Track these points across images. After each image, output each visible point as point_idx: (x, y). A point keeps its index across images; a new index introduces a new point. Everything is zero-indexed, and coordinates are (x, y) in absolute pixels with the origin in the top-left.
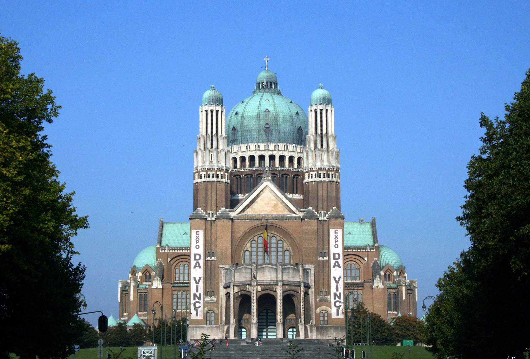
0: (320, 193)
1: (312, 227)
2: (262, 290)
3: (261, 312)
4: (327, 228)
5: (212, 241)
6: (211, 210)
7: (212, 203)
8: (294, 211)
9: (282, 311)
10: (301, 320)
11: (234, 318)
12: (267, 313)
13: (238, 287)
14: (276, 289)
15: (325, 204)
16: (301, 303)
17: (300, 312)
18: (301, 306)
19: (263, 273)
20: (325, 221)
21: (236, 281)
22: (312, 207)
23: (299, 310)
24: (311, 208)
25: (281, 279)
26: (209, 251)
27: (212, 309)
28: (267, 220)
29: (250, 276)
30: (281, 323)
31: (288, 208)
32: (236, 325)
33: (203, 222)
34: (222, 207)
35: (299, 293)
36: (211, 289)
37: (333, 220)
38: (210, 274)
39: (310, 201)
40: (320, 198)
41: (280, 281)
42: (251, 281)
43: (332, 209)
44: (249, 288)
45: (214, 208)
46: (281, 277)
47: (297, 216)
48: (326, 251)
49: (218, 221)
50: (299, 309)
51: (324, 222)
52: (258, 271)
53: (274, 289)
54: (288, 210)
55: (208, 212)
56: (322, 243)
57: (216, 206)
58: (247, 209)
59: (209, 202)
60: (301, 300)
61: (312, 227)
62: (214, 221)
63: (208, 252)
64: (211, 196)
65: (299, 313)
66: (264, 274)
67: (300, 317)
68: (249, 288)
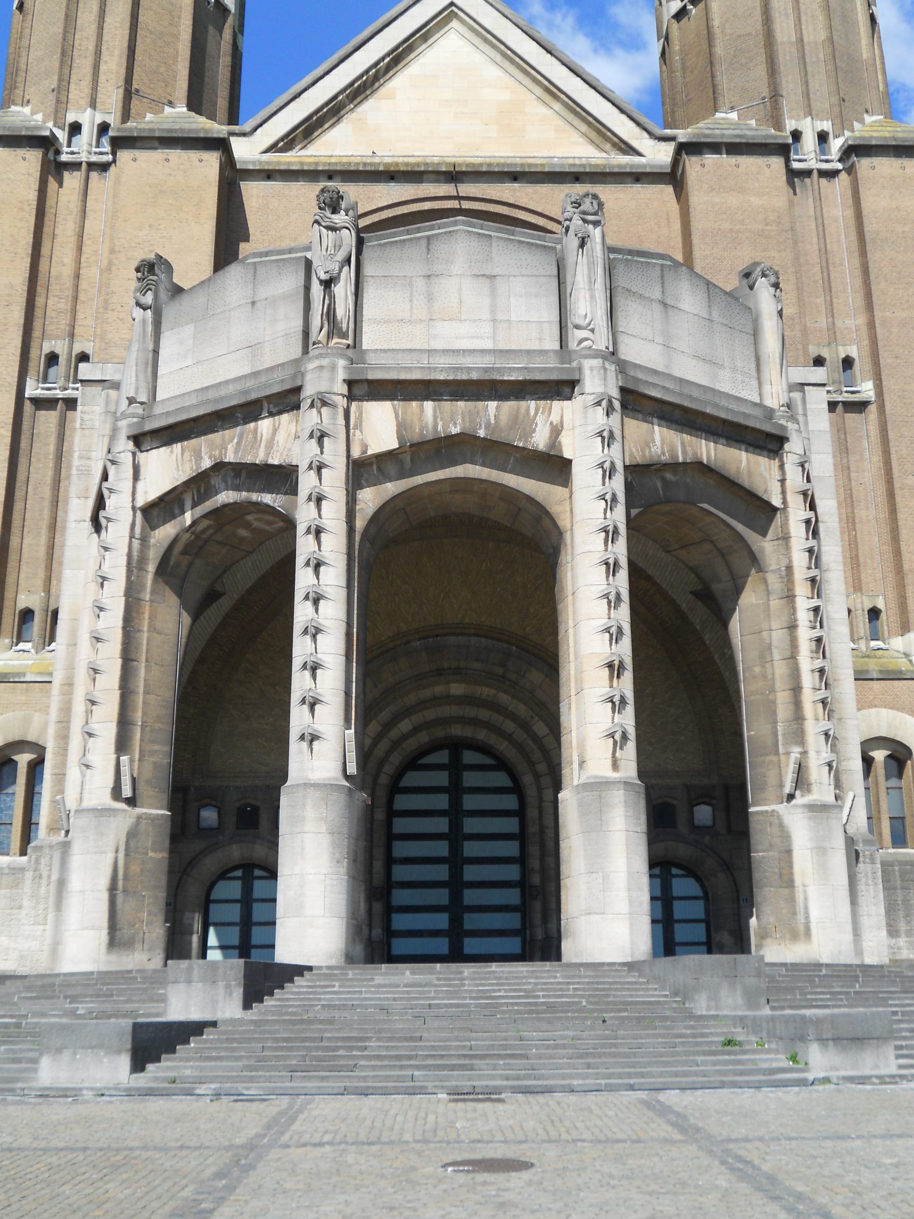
0: (784, 30)
1: (756, 201)
2: (415, 436)
3: (413, 764)
4: (850, 213)
5: (83, 285)
6: (93, 105)
7: (103, 67)
8: (625, 137)
9: (625, 647)
10: (801, 770)
11: (122, 744)
12: (456, 768)
13: (177, 447)
14: (556, 431)
15: (820, 84)
16: (790, 597)
17: (796, 690)
18: (792, 627)
19: (420, 283)
20: (831, 174)
21: (159, 397)
22: (732, 108)
23: (780, 669)
24: (734, 116)
25: (602, 341)
26: (60, 347)
27: (31, 738)
28: (454, 175)
29: (299, 323)
30: (627, 784)
31: (584, 128)
32: (139, 818)
33: (23, 164)
34: (171, 104)
35: (768, 504)
36: (47, 589)
37: (885, 166)
38: (47, 492)
39: (724, 81)
40: (786, 56)
41: (597, 354)
42: (296, 362)
43: (862, 121)
44: (275, 430)
45: (111, 96)
46: (601, 321)
47: (643, 160)
48: (853, 352)
49: (124, 155)
50: (776, 655)
51: (823, 181)
52: (369, 270)
53: (529, 432)
54: (584, 134)
55: (71, 118)
56: (820, 301)
57: (129, 80)
58: (332, 126)
59: (83, 65)
60: (789, 568)
61: (756, 201)
62: (104, 167)
63: (46, 349)
64: (100, 28)
65: (783, 698)
66: (430, 298)
67: (798, 736)
68: (275, 430)
